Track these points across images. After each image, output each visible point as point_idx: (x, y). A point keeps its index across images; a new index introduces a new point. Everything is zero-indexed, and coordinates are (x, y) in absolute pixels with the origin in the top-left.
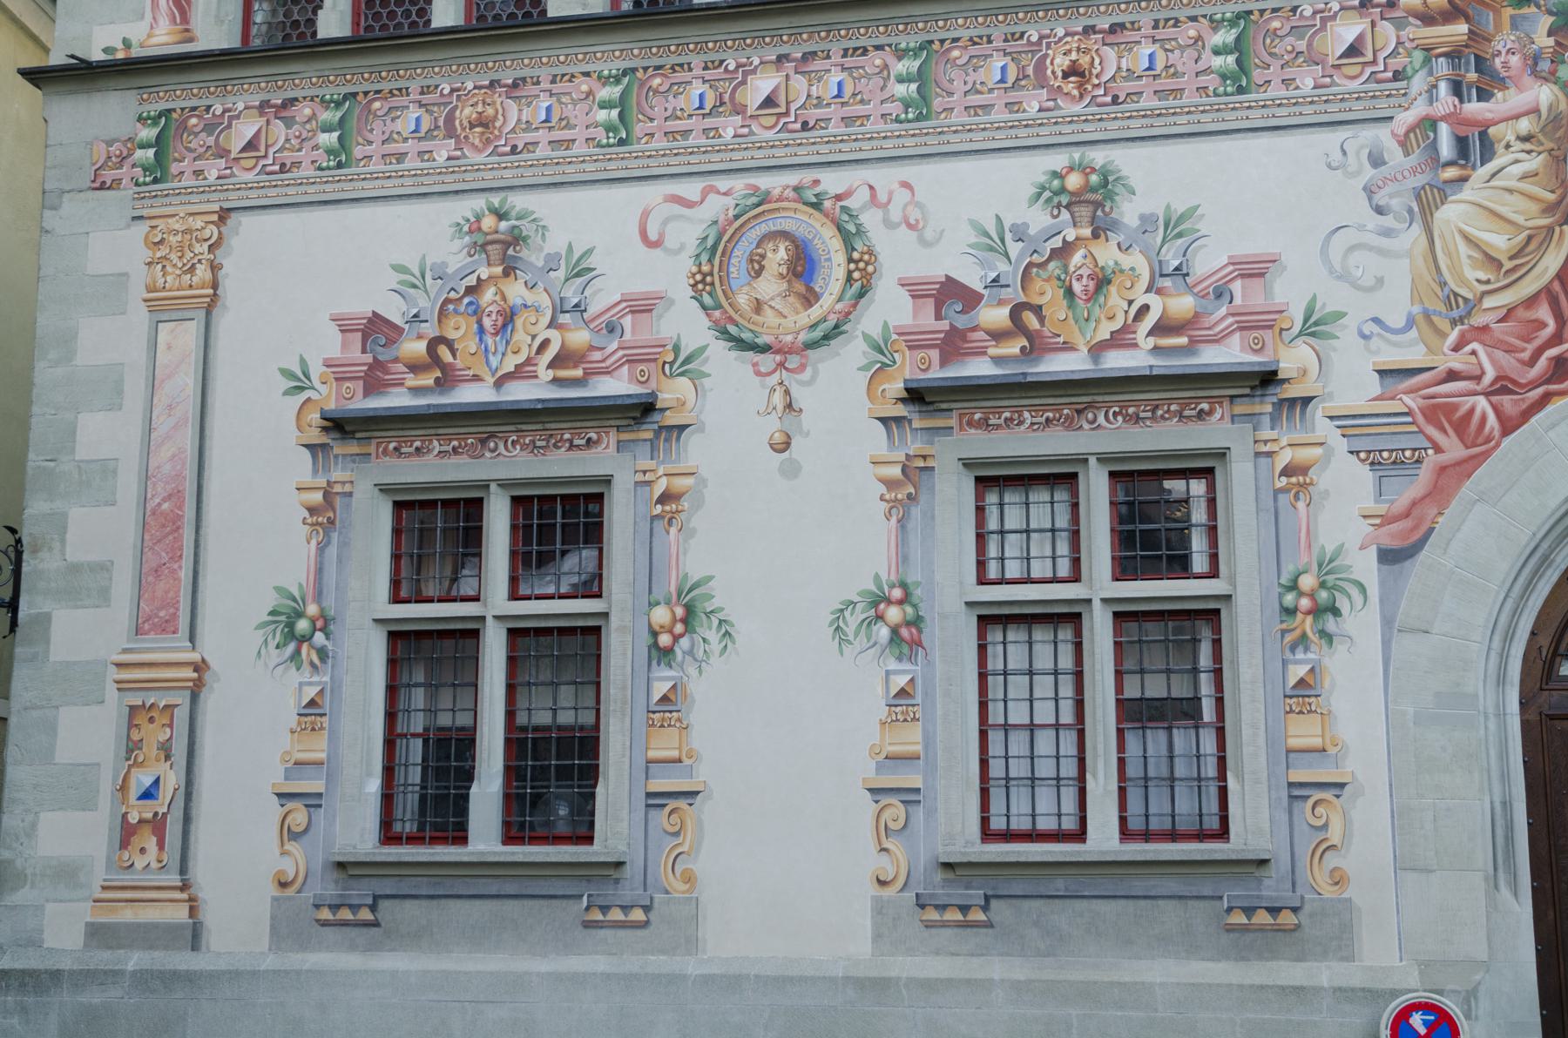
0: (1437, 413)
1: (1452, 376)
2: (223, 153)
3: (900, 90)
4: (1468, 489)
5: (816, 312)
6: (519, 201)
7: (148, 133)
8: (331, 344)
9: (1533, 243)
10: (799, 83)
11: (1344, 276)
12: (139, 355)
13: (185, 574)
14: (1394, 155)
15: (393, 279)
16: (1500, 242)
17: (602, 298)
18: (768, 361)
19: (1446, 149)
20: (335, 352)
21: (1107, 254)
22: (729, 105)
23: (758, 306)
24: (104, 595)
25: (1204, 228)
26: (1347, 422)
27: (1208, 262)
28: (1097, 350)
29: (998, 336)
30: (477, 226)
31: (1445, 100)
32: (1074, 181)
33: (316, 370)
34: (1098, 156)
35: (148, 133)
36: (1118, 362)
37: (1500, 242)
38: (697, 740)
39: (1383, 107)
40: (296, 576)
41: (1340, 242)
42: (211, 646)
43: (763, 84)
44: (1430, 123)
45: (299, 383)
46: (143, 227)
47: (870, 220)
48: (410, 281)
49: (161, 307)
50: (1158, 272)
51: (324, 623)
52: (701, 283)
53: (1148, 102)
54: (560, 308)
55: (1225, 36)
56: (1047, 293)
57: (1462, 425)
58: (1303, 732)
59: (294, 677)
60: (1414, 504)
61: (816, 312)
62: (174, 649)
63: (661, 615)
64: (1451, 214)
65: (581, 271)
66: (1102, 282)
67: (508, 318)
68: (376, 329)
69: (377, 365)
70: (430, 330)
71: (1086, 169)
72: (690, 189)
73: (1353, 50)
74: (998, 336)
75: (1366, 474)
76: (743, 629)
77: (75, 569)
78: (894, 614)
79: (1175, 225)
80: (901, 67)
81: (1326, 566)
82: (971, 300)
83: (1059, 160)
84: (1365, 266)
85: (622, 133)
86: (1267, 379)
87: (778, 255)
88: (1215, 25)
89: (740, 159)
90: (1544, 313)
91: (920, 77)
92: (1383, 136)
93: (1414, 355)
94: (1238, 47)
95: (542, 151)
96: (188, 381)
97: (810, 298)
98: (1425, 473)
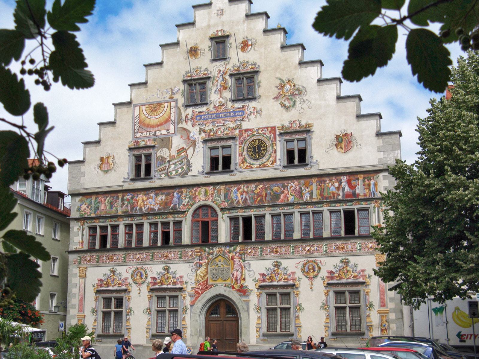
0: (196, 292)
1: (197, 288)
2: (86, 261)
3: (151, 257)
4: (198, 300)
5: (142, 280)
6: (115, 267)
7: (79, 258)
8: (97, 282)
9: (205, 275)
10: (141, 256)
11: (189, 278)
12: (78, 282)
13: (83, 306)
14: (194, 266)
15: (103, 275)
16: (202, 275)
17: (123, 278)
18: (138, 285)
19: (198, 266)
20: (97, 283)
21: (169, 275)
22: (135, 258)
23: (137, 279)
24: (75, 308)
25: (177, 273)
26: (189, 293)
27: (177, 276)
28: (167, 285)
29: (159, 283)
30: (111, 270)
31: (198, 261)
32: (166, 267)
33: (95, 285)
34: (168, 265)
35: (79, 258)
36: (170, 286)
37: (202, 275)
38: (131, 323)
39: (193, 261)
40: (94, 306)
41: (189, 275)
42: (86, 313)
43: (138, 256)
44: (197, 263)
45: (94, 286)
46: (78, 269)
47: (147, 271)
48: (104, 275)
49: (81, 277)
50: (173, 277)
51: (96, 311)
52: (132, 277)
53: (173, 260)
54: (119, 279)
55: (179, 253)
56: (163, 279)
57: (198, 293)
58: (183, 323)
59: (94, 317)
60: (194, 301)
61: (142, 280)
62: (82, 313)
63: (128, 311)
64: (198, 272)
65: (120, 275)
66: (168, 278)
67: (114, 279)
68: (101, 280)
69: (101, 284)
70: (106, 281)
71: (167, 266)
72: (131, 267)
73: (191, 255)
74: (159, 283)
75: (190, 298)
76: (135, 312)
77: (72, 305)
78: (149, 311)
79: (175, 272)
80: (151, 255)
81: (186, 306)
82: (156, 279)
83: (164, 265)
84: (191, 277)
85: (125, 260)
86: (181, 289)
87: (139, 274)
88: (179, 252)
89: (136, 264)
90: (205, 282)
91: (152, 256)
92: (193, 264)
93: (194, 286)
94: (181, 254)
95: (117, 262)
96: (83, 285)
97: (142, 279)
98: (195, 298)
